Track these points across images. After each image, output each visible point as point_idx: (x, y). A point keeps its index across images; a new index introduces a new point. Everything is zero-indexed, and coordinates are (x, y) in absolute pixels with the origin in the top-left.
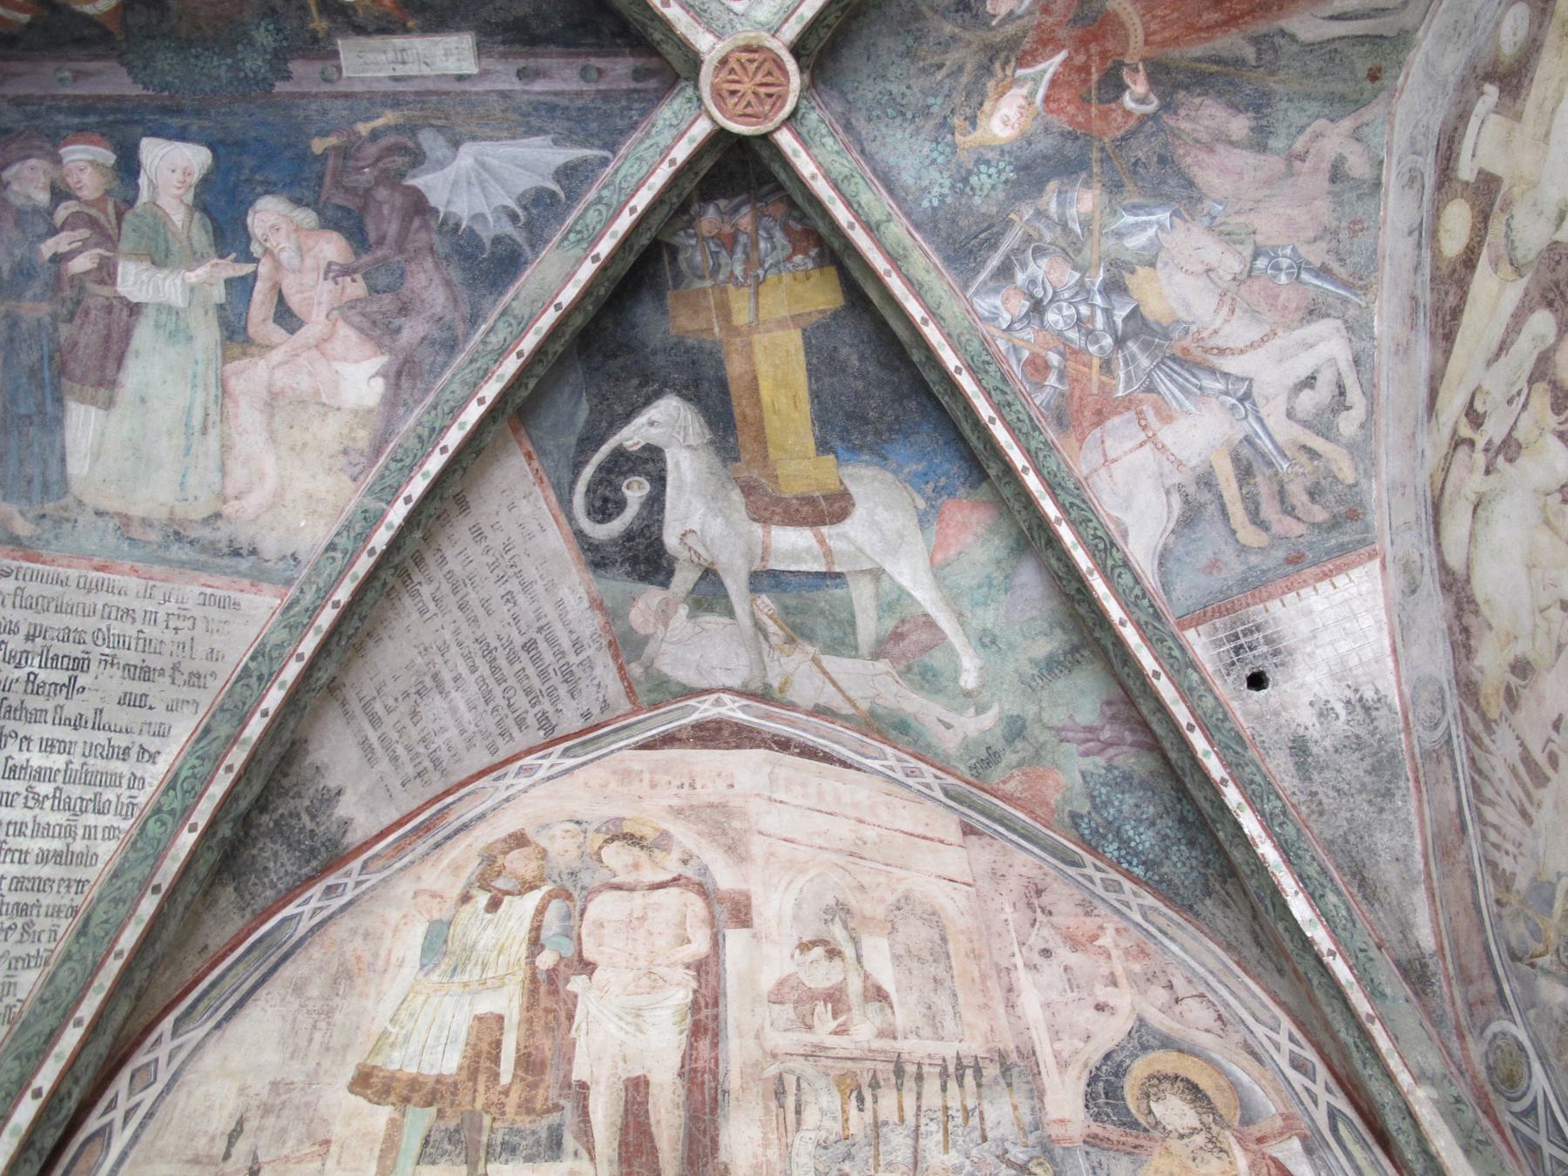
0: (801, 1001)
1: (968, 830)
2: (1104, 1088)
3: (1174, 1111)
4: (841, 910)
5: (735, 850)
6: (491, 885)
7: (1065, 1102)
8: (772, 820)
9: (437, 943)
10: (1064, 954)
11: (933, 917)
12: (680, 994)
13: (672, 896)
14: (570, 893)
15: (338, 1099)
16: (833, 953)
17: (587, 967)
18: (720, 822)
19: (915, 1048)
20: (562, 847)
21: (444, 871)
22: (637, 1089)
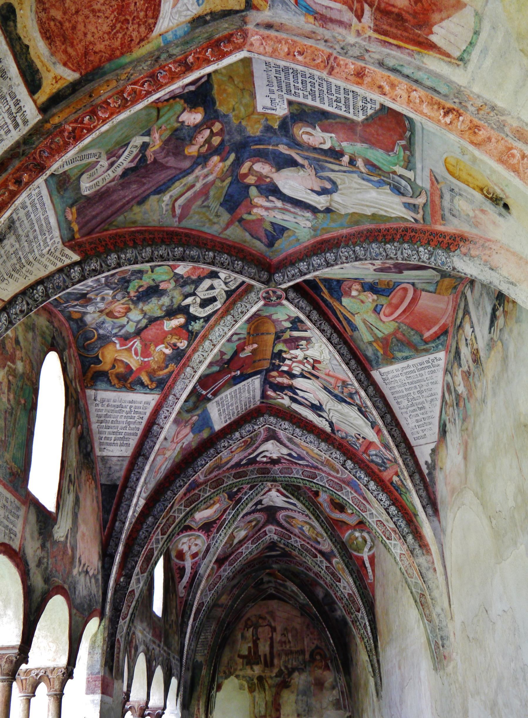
0: (282, 643)
1: (302, 615)
2: (312, 655)
3: (318, 657)
4: (286, 629)
5: (274, 620)
6: (247, 627)
7: (307, 656)
8: (278, 614)
9: (243, 637)
10: (310, 635)
11: (296, 630)
12: (269, 643)
13: (267, 627)
14: (256, 627)
15: (237, 658)
16: (285, 636)
17: (259, 639)
18: (272, 614)
19: (293, 649)
20: (254, 619)
21: (241, 625)
22: (265, 656)
